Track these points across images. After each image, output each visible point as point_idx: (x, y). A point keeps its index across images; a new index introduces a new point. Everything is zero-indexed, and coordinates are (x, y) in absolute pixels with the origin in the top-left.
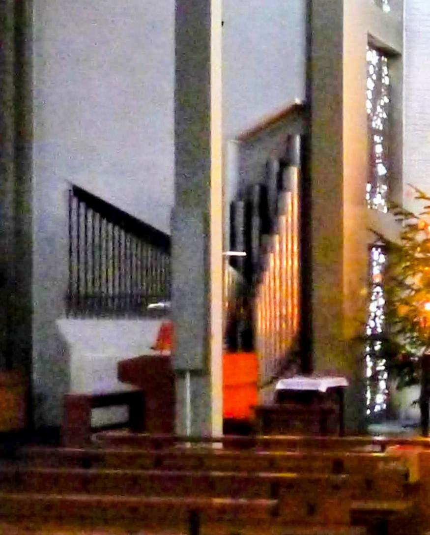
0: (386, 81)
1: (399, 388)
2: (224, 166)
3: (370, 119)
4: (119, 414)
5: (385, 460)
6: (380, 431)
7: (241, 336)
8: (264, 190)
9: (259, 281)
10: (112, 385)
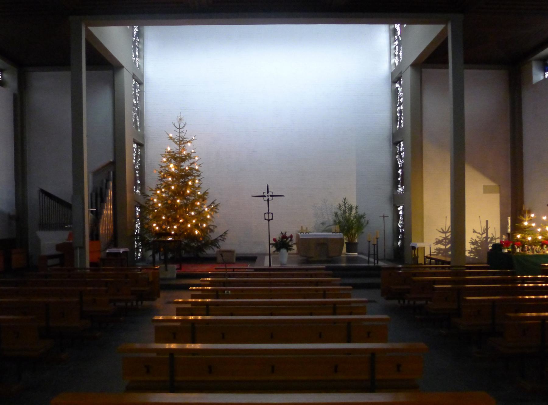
0: (139, 153)
1: (146, 251)
2: (88, 181)
3: (134, 166)
4: (56, 261)
5: (141, 274)
6: (140, 265)
7: (95, 236)
8: (101, 189)
9: (100, 218)
10: (54, 252)
